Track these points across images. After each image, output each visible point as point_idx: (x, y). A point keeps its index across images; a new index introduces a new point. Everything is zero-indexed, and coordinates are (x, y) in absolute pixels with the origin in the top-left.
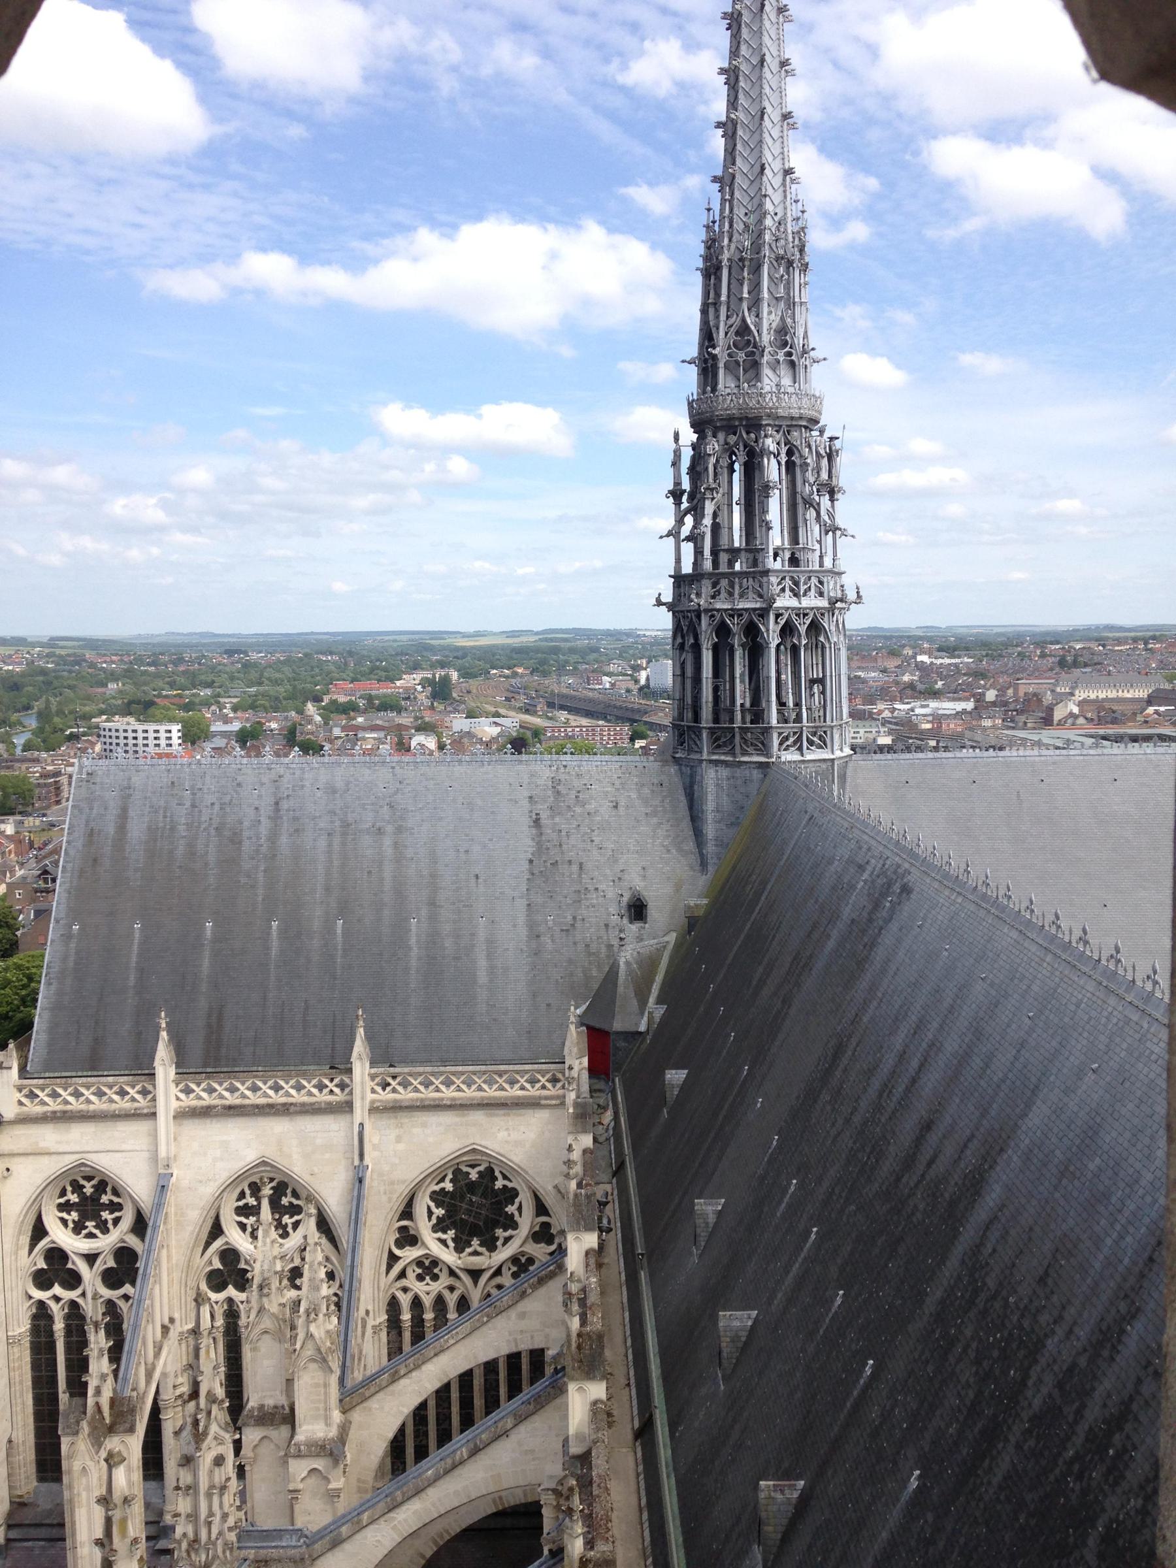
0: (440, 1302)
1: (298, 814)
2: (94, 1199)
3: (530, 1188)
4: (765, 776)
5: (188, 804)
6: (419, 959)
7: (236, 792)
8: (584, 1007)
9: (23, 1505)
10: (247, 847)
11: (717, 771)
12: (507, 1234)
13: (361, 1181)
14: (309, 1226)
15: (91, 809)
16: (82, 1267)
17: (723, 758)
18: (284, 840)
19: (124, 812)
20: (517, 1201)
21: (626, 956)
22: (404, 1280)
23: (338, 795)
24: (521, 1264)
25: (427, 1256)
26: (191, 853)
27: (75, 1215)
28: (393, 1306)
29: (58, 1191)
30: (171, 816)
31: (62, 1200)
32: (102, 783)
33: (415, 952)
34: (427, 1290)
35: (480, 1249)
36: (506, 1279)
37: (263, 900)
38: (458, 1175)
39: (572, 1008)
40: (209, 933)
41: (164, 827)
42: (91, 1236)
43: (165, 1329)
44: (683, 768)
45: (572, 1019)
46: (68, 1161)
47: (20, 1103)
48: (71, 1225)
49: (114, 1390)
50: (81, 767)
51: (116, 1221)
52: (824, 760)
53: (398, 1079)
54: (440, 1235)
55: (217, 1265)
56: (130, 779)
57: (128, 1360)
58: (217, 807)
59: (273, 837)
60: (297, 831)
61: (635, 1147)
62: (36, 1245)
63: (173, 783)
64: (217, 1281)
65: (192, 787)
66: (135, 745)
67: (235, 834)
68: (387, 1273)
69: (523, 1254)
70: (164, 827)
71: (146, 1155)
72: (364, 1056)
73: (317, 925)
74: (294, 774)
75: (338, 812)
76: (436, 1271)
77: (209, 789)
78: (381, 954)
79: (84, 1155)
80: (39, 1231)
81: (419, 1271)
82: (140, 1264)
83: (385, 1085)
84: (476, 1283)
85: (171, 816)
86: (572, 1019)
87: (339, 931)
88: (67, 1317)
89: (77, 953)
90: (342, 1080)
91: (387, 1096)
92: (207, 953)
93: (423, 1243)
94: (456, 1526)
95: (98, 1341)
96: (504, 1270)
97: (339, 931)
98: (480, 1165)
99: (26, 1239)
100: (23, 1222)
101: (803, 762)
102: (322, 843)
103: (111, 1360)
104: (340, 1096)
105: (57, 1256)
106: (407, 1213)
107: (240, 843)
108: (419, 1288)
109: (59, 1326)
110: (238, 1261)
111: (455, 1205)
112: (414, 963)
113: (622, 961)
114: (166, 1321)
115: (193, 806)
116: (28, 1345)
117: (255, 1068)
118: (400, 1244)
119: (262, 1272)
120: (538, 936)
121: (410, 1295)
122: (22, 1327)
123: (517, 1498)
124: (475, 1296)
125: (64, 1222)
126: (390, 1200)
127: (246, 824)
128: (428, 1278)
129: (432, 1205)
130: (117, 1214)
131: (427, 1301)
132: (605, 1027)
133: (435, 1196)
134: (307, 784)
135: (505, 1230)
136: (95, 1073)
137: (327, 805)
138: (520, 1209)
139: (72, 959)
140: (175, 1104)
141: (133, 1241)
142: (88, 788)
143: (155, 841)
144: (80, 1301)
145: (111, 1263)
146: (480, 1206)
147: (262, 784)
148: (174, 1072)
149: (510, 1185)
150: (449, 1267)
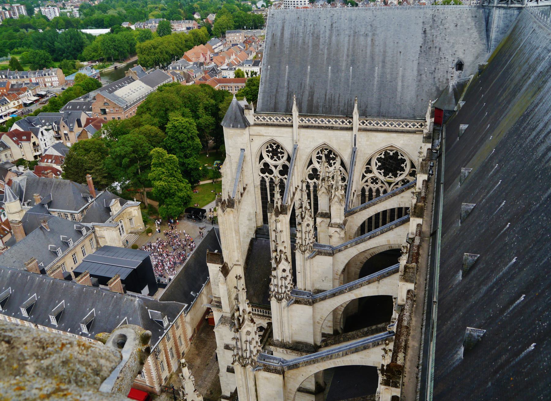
0: (378, 191)
1: (339, 28)
3: (410, 159)
4: (520, 13)
5: (303, 25)
6: (378, 81)
7: (318, 20)
8: (435, 101)
9: (260, 229)
10: (322, 40)
11: (499, 11)
12: (401, 173)
13: (354, 152)
14: (338, 165)
15: (273, 27)
16: (273, 169)
17: (503, 5)
18: (334, 38)
20: (405, 163)
21: (452, 83)
23: (353, 22)
24: (404, 182)
25: (374, 177)
26: (304, 42)
27: (271, 154)
28: (363, 190)
31: (267, 150)
33: (376, 79)
34: (374, 187)
36: (399, 186)
38: (386, 154)
39: (430, 101)
40: (309, 70)
41: (295, 34)
42: (275, 160)
43: (296, 189)
44: (486, 10)
45: (430, 104)
46: (268, 139)
48: (270, 157)
49: (282, 203)
50: (270, 13)
51: (282, 157)
52: (547, 6)
53: (368, 121)
56: (285, 16)
57: (286, 195)
58: (312, 26)
59: (330, 37)
60: (338, 35)
61: (446, 150)
64: (311, 177)
67: (318, 36)
68: (362, 180)
69: (406, 179)
70: (295, 34)
71: (291, 138)
73: (343, 68)
76: (377, 181)
78: (365, 79)
80: (261, 158)
82: (289, 170)
83: (363, 123)
84: (390, 186)
86: (430, 104)
87: (351, 71)
88: (270, 182)
89: (270, 75)
91: (364, 126)
92: (308, 77)
94: (377, 251)
95: (277, 189)
96: (399, 183)
97: (351, 71)
99: (258, 159)
101: (538, 6)
102: (347, 39)
103: (281, 195)
104: (349, 125)
105: (266, 165)
106: (369, 163)
107: (319, 39)
108: (372, 186)
109: (268, 184)
112: (376, 83)
113: (451, 85)
115: (305, 26)
118: (366, 172)
119: (323, 176)
120: (421, 75)
121: (369, 187)
122: (258, 183)
123: (396, 247)
124: (389, 190)
125: (268, 156)
127: (322, 32)
129: (377, 162)
130: (283, 155)
131: (374, 190)
132: (442, 108)
133: (378, 159)
134: (342, 17)
135: (400, 172)
138: (406, 166)
139: (268, 77)
140: (298, 124)
141: (287, 163)
143: (293, 38)
144: (273, 178)
145: (281, 169)
147: (327, 18)
149: (403, 158)
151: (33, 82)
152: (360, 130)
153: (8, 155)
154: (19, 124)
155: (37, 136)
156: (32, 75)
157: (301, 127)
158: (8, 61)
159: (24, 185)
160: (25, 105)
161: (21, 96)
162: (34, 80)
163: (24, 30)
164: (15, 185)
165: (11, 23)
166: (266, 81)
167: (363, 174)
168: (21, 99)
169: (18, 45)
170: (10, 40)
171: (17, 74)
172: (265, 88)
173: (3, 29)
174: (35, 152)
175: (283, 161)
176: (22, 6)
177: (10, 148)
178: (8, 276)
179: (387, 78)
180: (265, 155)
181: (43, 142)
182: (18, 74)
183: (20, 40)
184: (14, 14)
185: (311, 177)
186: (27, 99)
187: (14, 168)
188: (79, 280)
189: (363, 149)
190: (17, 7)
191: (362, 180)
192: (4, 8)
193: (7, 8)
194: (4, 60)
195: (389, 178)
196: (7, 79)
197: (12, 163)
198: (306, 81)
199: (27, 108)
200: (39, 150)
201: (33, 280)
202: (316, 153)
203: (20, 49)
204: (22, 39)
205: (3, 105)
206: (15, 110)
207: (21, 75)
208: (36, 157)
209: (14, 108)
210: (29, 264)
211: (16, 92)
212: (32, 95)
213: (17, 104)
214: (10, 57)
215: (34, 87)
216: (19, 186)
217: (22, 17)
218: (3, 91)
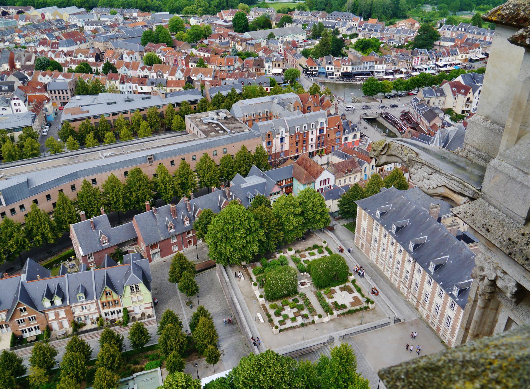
151: (487, 40)
153: (441, 102)
154: (464, 77)
155: (474, 93)
156: (489, 34)
159: (452, 135)
160: (471, 60)
161: (471, 51)
162: (488, 39)
164: (445, 133)
178: (412, 209)
181: (476, 100)
182: (476, 30)
187: (441, 115)
188: (472, 247)
194: (467, 14)
199: (471, 63)
201: (430, 224)
203: (485, 6)
207: (479, 31)
208: (463, 112)
209: (460, 60)
210: (433, 208)
213: (464, 58)
214: (475, 12)
216: (449, 134)
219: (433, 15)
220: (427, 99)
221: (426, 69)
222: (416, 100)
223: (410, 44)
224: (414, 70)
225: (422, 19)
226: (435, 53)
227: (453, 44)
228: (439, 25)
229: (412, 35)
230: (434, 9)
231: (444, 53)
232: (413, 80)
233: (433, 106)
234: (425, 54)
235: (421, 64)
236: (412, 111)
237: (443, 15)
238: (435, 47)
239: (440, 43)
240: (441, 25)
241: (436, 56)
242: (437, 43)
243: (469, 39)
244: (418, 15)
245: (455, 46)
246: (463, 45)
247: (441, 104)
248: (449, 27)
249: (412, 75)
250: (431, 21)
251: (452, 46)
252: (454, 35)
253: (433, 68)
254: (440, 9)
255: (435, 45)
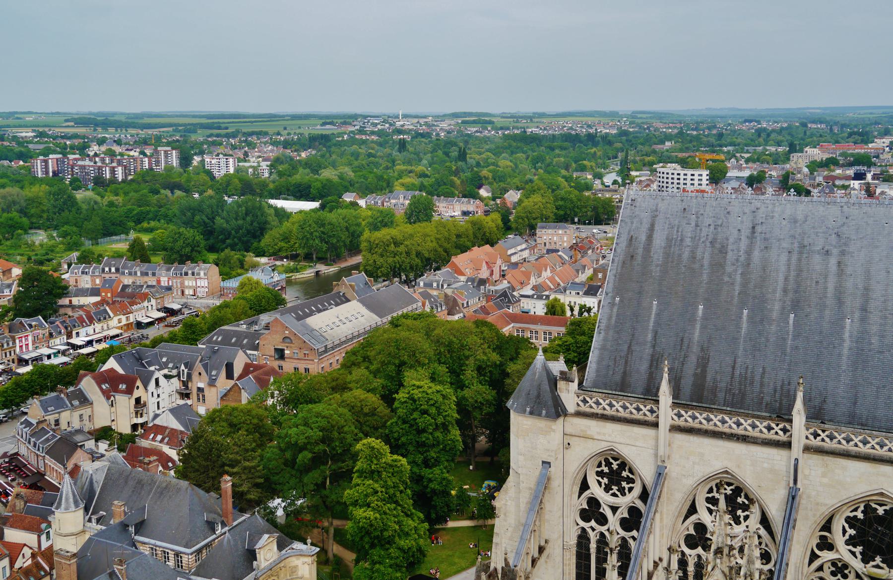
1: (768, 236)
2: (617, 473)
5: (693, 224)
6: (850, 349)
7: (726, 218)
10: (730, 254)
13: (793, 498)
14: (754, 522)
15: (632, 223)
16: (608, 513)
18: (756, 254)
19: (652, 228)
22: (821, 572)
23: (798, 224)
25: (840, 560)
26: (693, 257)
27: (605, 480)
29: (597, 463)
30: (682, 232)
31: (599, 469)
32: (640, 207)
33: (847, 344)
35: (881, 565)
37: (739, 294)
38: (868, 509)
42: (614, 495)
43: (656, 565)
46: (602, 446)
47: (578, 405)
48: (603, 486)
50: (628, 196)
51: (630, 489)
53: (827, 433)
54: (850, 547)
55: (692, 531)
56: (657, 205)
58: (712, 227)
59: (749, 253)
60: (766, 248)
62: (582, 493)
63: (685, 209)
64: (691, 542)
65: (697, 213)
66: (663, 182)
67: (723, 247)
68: (809, 564)
71: (652, 451)
72: (803, 412)
73: (775, 315)
74: (767, 207)
75: (797, 236)
76: (846, 572)
77: (708, 215)
79: (614, 444)
80: (584, 486)
81: (834, 569)
82: (643, 520)
83: (816, 435)
85: (682, 232)
87: (791, 322)
88: (598, 542)
89: (617, 315)
90: (785, 426)
91: (817, 442)
92: (698, 326)
93: (837, 551)
95: (613, 560)
97: (791, 322)
98: (886, 505)
99: (577, 489)
100: (576, 477)
102: (784, 258)
104: (782, 437)
105: (594, 502)
106: (827, 526)
107: (726, 253)
109: (593, 546)
110: (706, 533)
111: (865, 530)
112: (845, 351)
114: (657, 560)
115: (697, 226)
116: (575, 552)
117: (725, 408)
118: (820, 547)
122: (573, 541)
125: (600, 483)
126: (814, 515)
127: (731, 240)
128: (839, 575)
129: (847, 526)
130: (631, 485)
133: (848, 520)
134: (776, 215)
136: (623, 394)
137: (789, 231)
139: (614, 319)
140: (671, 422)
141: (639, 504)
142: (632, 210)
143: (670, 247)
144: (606, 533)
145: (626, 515)
146: (884, 534)
147: (744, 213)
148: (671, 401)
150: (857, 573)
151: (162, 284)
152: (807, 449)
153: (86, 417)
154: (119, 360)
155: (146, 387)
156: (164, 272)
157: (675, 429)
158: (128, 243)
159: (99, 479)
160: (139, 325)
161: (135, 307)
162: (164, 281)
163: (168, 192)
164: (84, 479)
165: (148, 178)
166: (608, 327)
167: (812, 550)
168: (134, 313)
169: (151, 215)
170: (140, 206)
171: (138, 268)
172: (605, 340)
173: (132, 187)
174: (137, 417)
175: (631, 498)
176: (174, 152)
177: (92, 404)
179: (871, 344)
180: (592, 480)
181: (155, 400)
183: (156, 208)
184: (158, 163)
185: (691, 542)
186: (144, 315)
187: (90, 444)
189: (814, 493)
190: (166, 152)
191: (809, 564)
192: (142, 153)
193: (148, 152)
194: (120, 241)
195: (874, 566)
196: (118, 275)
197: (89, 433)
198: (693, 334)
199: (140, 331)
200: (144, 415)
202: (707, 489)
203: (153, 224)
204: (161, 207)
205: (100, 320)
206: (118, 332)
207: (143, 269)
208: (135, 427)
209: (117, 328)
211: (129, 300)
212: (154, 308)
213: (124, 322)
214: (133, 235)
215: (162, 293)
216: (91, 480)
217: (169, 169)
218: (106, 295)
219: (52, 249)
220: (51, 418)
221: (49, 357)
222: (28, 424)
223: (7, 312)
224: (22, 362)
225: (29, 259)
226: (63, 322)
227: (98, 299)
228: (66, 267)
229: (6, 292)
230: (51, 237)
231: (81, 319)
232: (17, 384)
233: (69, 429)
234: (40, 326)
235: (36, 348)
236: (23, 451)
237: (70, 248)
238: (62, 311)
239: (70, 301)
240: (69, 265)
241: (66, 328)
242: (65, 301)
243: (128, 286)
244: (19, 251)
245: (103, 302)
246: (119, 299)
247: (86, 422)
248: (84, 268)
249: (19, 374)
250: (49, 260)
251: (95, 304)
252: (98, 281)
253: (64, 353)
254: (64, 235)
255: (62, 306)
